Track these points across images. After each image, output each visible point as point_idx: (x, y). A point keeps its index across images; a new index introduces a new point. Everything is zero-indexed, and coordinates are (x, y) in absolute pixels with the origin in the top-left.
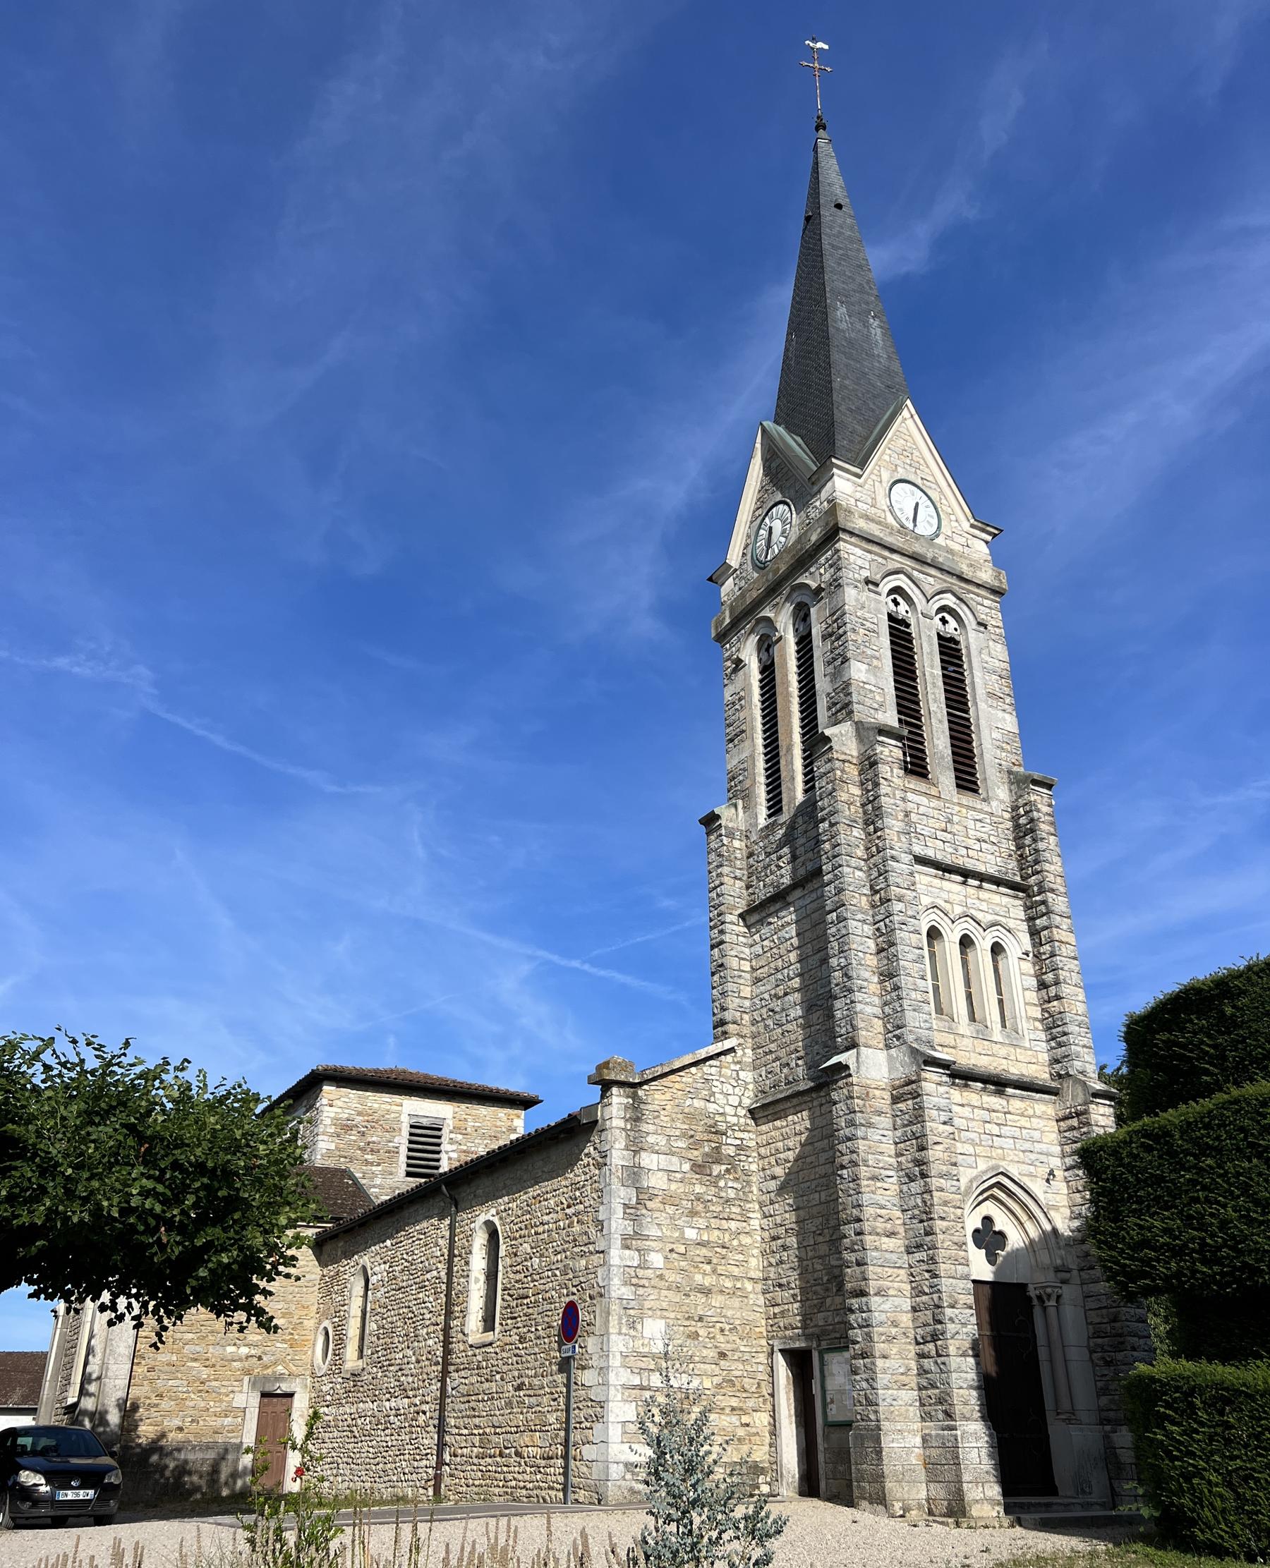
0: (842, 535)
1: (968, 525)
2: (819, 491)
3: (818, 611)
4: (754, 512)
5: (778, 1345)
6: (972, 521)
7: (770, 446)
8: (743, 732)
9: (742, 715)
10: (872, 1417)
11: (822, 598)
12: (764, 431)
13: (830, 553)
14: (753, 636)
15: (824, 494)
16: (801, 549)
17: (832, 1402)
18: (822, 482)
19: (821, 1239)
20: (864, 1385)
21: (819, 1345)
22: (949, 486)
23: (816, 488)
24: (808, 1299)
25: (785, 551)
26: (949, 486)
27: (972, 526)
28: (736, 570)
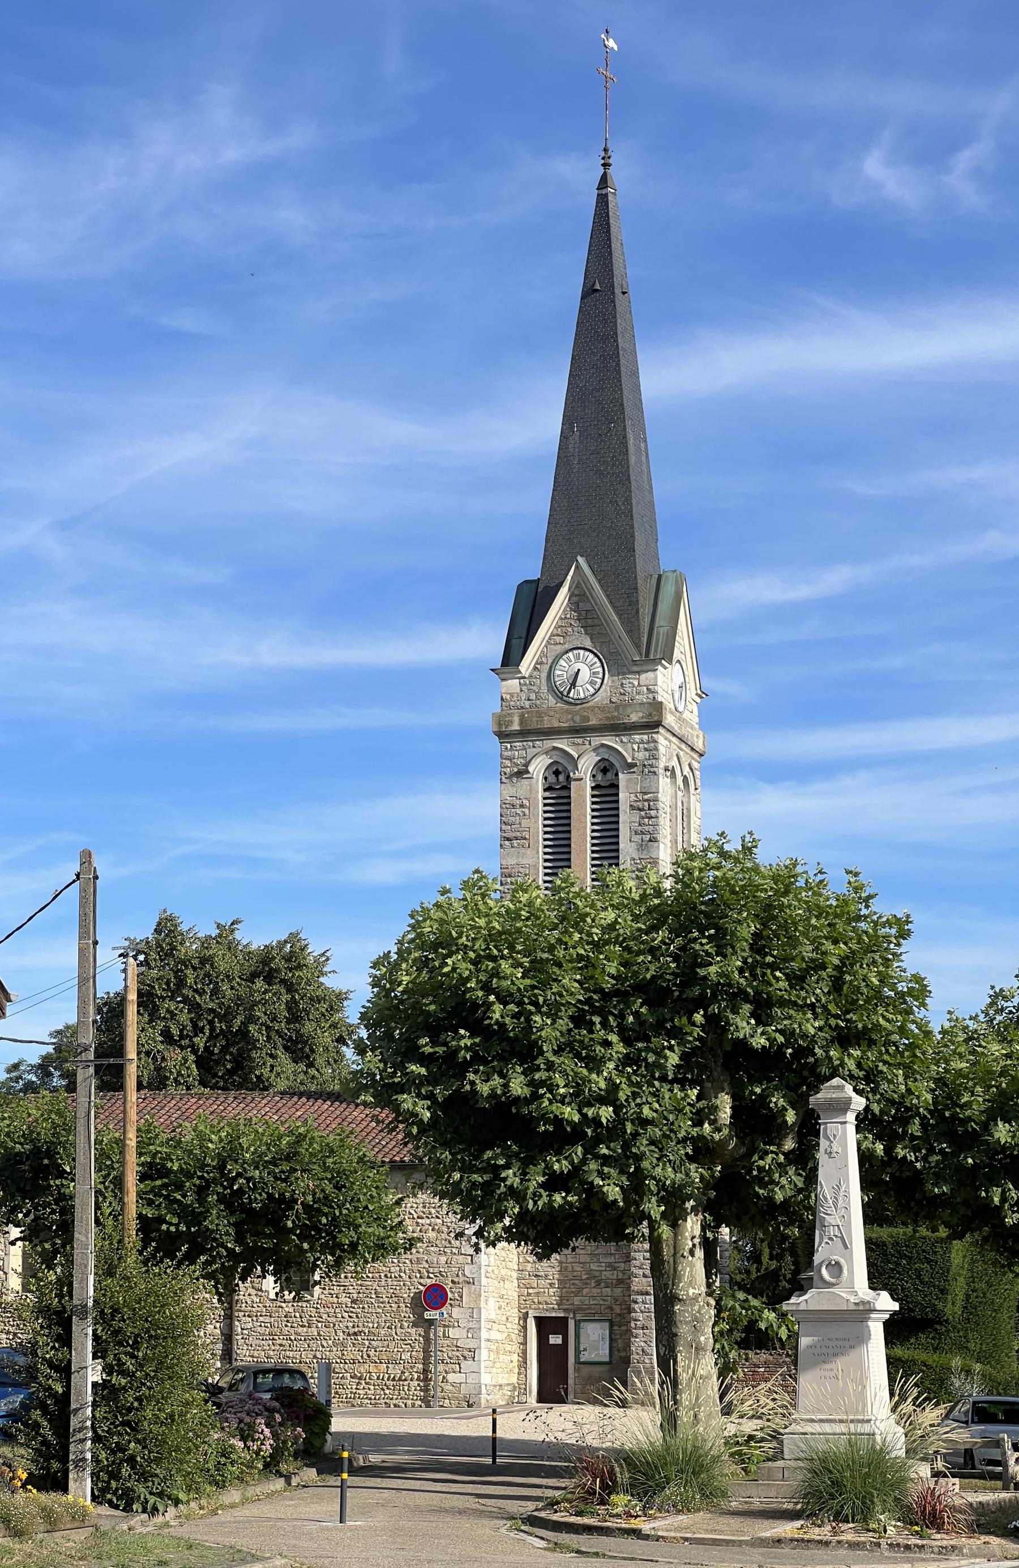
0: (661, 730)
1: (695, 692)
2: (639, 673)
3: (629, 781)
4: (552, 635)
5: (532, 1314)
6: (699, 692)
7: (579, 583)
8: (525, 839)
9: (525, 823)
10: (647, 1361)
11: (634, 772)
12: (578, 567)
13: (645, 737)
14: (544, 756)
15: (646, 678)
16: (618, 718)
17: (585, 1350)
18: (644, 668)
19: (583, 1252)
20: (643, 1344)
21: (574, 1316)
22: (692, 657)
23: (635, 668)
24: (565, 1288)
25: (602, 709)
26: (692, 657)
27: (697, 694)
28: (525, 678)
